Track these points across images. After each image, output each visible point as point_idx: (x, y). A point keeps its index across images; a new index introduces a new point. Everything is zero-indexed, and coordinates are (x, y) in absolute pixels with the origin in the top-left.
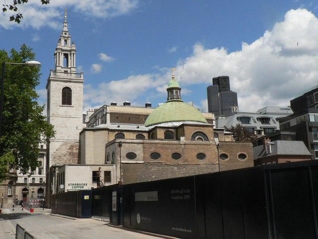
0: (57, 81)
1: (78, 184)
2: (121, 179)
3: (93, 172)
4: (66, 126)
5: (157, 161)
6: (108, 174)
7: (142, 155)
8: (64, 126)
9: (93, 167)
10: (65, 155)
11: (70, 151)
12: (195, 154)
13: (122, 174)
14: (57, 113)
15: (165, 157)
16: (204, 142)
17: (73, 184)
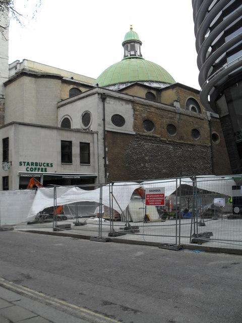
1: (36, 164)
2: (104, 158)
5: (150, 133)
6: (85, 148)
7: (132, 120)
12: (190, 129)
13: (107, 149)
15: (160, 129)
16: (196, 114)
17: (28, 164)
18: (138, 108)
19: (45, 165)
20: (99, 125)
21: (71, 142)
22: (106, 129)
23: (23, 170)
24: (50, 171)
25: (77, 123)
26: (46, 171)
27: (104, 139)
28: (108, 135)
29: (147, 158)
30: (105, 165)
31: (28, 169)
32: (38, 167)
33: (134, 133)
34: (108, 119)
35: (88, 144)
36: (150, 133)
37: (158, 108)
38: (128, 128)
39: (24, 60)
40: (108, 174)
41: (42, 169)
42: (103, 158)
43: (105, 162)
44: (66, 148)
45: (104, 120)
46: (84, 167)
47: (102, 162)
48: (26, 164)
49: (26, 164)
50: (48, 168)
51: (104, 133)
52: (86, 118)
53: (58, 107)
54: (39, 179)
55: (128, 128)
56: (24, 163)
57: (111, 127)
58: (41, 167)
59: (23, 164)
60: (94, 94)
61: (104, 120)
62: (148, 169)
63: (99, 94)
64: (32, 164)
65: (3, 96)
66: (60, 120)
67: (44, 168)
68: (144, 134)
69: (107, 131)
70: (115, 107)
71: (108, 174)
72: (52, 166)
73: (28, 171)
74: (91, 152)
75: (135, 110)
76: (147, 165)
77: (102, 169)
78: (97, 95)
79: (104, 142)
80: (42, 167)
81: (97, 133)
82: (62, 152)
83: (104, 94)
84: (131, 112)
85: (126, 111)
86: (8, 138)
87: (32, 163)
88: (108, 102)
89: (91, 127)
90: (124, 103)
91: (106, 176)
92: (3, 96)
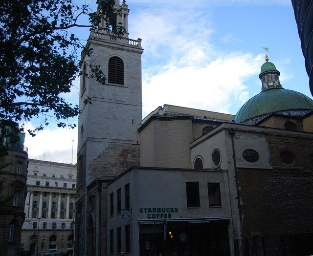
0: (101, 45)
1: (159, 210)
2: (238, 198)
3: (187, 183)
4: (115, 117)
6: (214, 188)
8: (112, 117)
9: (186, 173)
10: (113, 166)
11: (122, 159)
13: (240, 188)
14: (101, 95)
18: (272, 140)
19: (168, 210)
20: (229, 162)
21: (197, 184)
22: (237, 166)
23: (144, 217)
24: (175, 217)
25: (208, 163)
26: (170, 216)
27: (236, 177)
28: (240, 173)
29: (289, 194)
30: (239, 206)
31: (150, 216)
32: (162, 213)
33: (271, 168)
34: (239, 154)
35: (218, 184)
36: (291, 166)
37: (297, 138)
38: (264, 162)
39: (165, 105)
40: (243, 216)
41: (166, 215)
42: (236, 198)
43: (239, 203)
44: (192, 190)
45: (234, 156)
46: (215, 209)
47: (235, 202)
48: (147, 210)
49: (147, 210)
50: (172, 213)
51: (236, 170)
52: (216, 156)
53: (191, 149)
54: (162, 225)
55: (264, 162)
56: (145, 209)
57: (243, 164)
58: (164, 213)
59: (144, 210)
60: (221, 130)
61: (234, 156)
62: (292, 207)
63: (225, 129)
64: (154, 210)
65: (137, 142)
66: (193, 161)
67: (168, 213)
68: (283, 168)
69: (238, 168)
70: (245, 142)
71: (243, 216)
72: (176, 211)
73: (150, 218)
74: (221, 192)
75: (270, 143)
76: (290, 202)
77: (237, 210)
78: (224, 131)
79: (236, 181)
80: (166, 212)
81: (227, 171)
82: (187, 195)
83: (232, 129)
84: (266, 145)
85: (259, 144)
86: (129, 184)
87: (153, 209)
88: (237, 137)
89: (221, 165)
90: (256, 136)
91: (241, 217)
92: (137, 142)
